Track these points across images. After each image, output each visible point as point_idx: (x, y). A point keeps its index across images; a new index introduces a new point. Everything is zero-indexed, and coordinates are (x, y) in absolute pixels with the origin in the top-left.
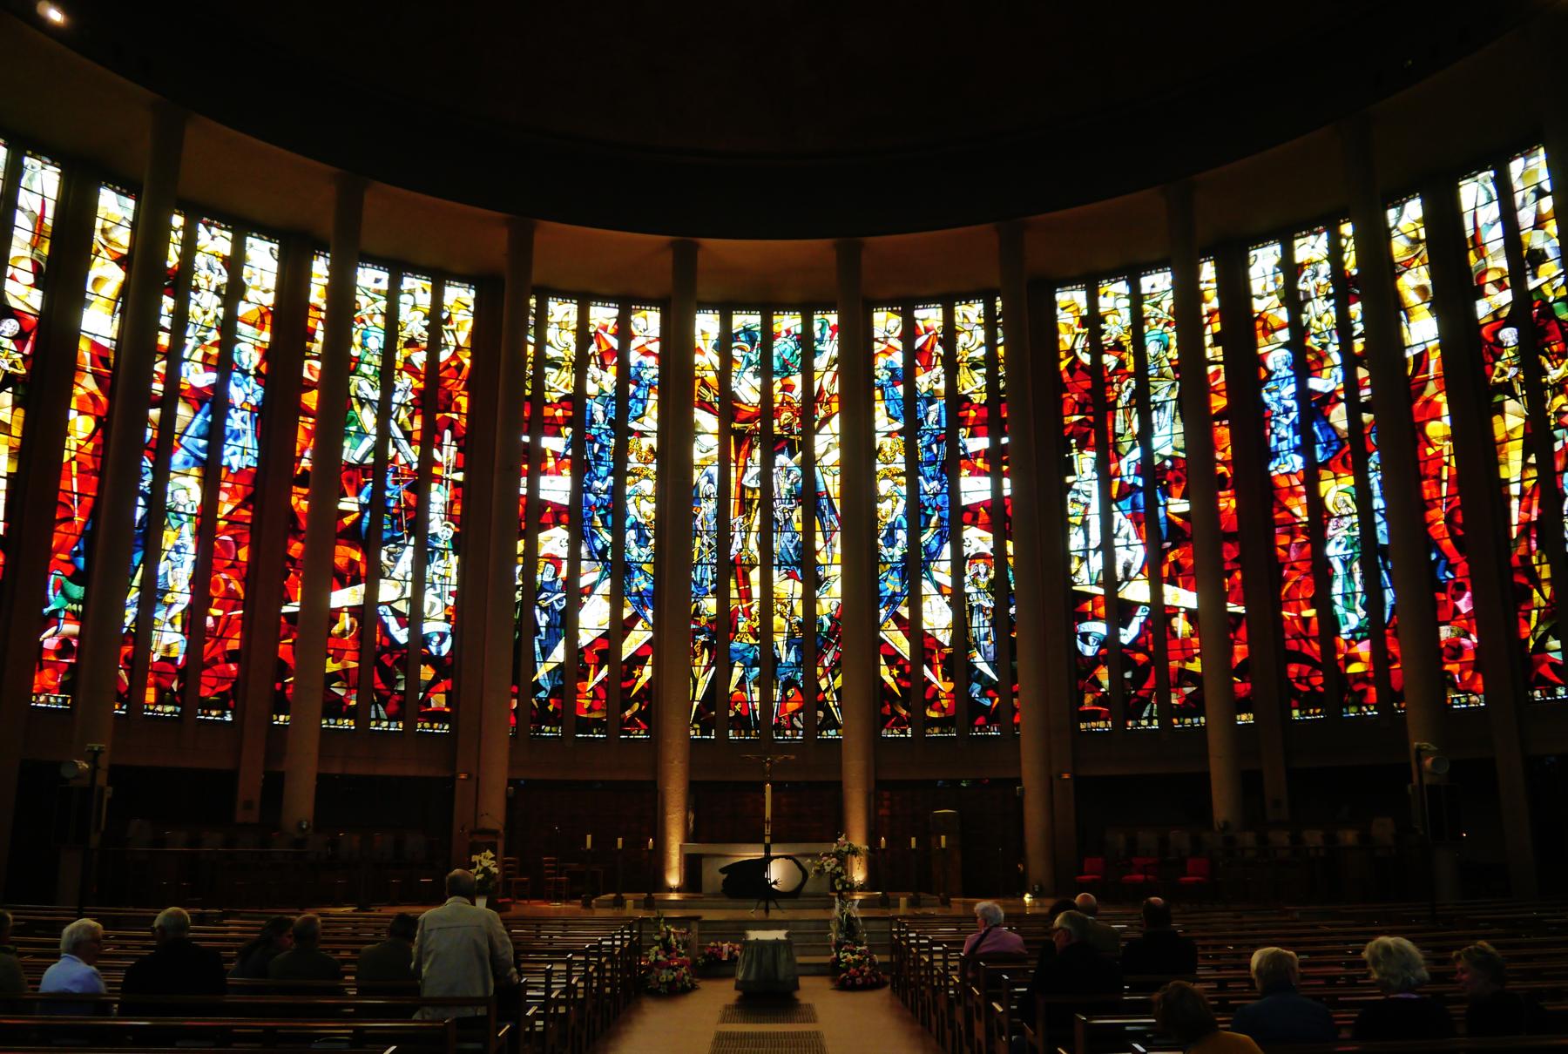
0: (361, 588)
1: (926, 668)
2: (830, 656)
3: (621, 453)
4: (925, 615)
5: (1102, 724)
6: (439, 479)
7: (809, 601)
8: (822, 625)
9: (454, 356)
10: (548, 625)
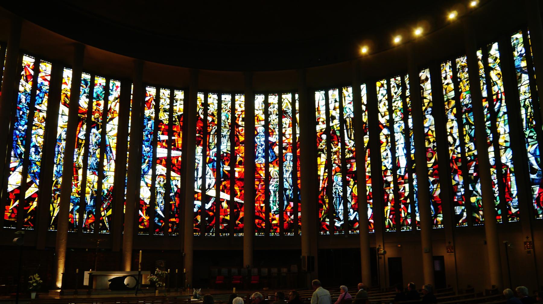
1: (140, 211)
2: (106, 203)
3: (31, 117)
4: (141, 193)
5: (197, 234)
7: (100, 183)
8: (104, 193)
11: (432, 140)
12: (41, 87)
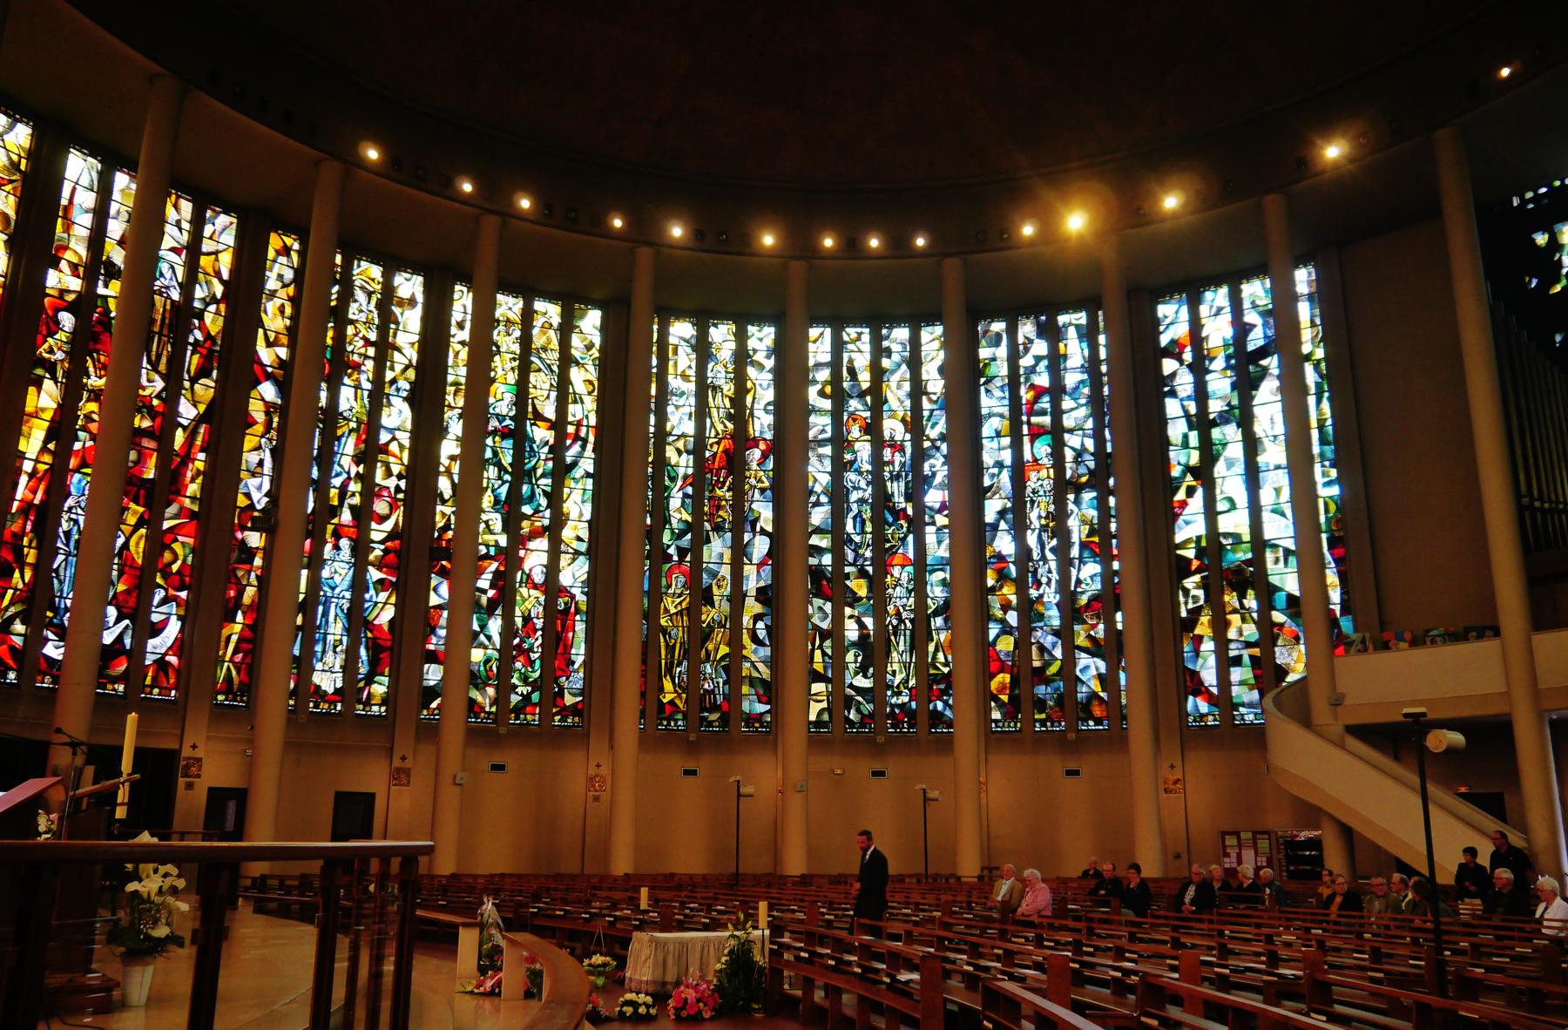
11: (396, 469)
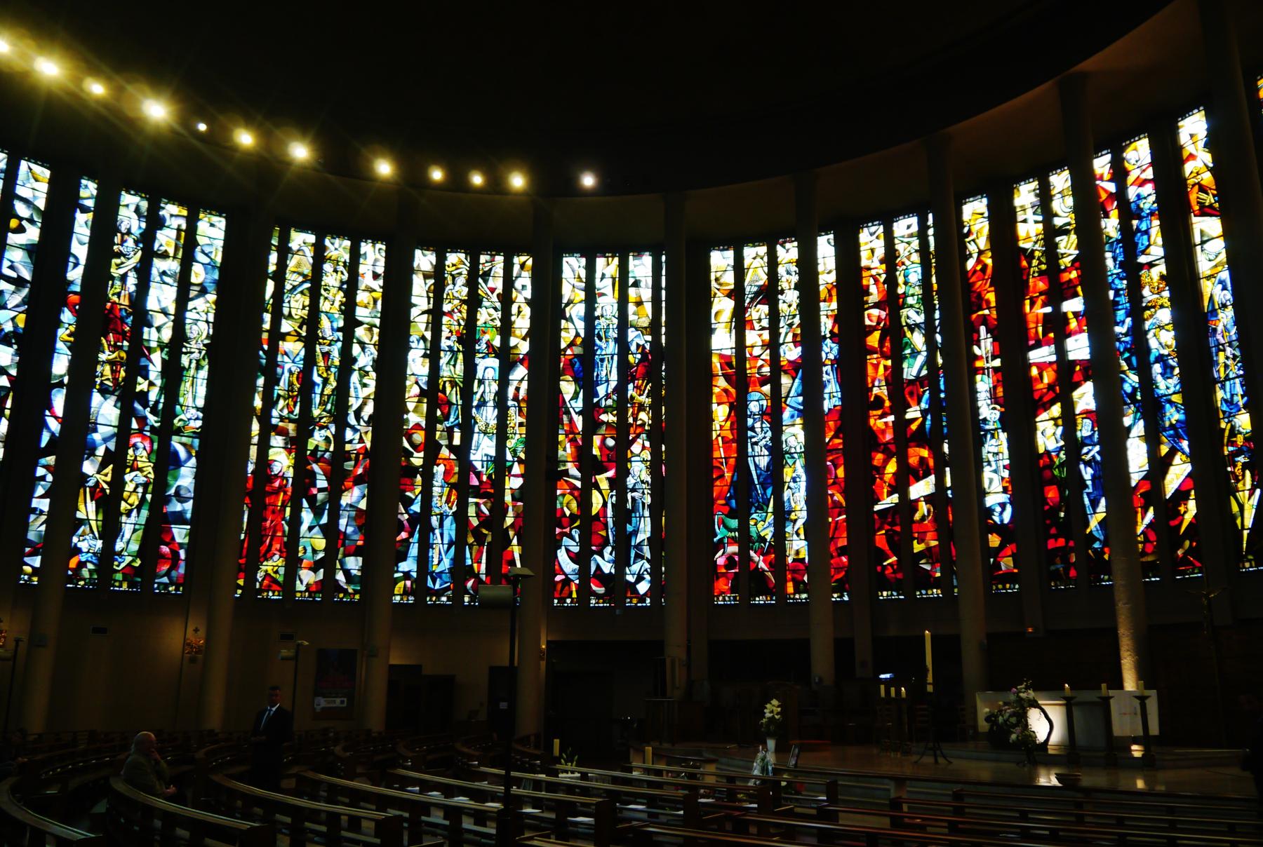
0: (932, 478)
6: (982, 370)
9: (979, 261)
10: (1094, 478)
12: (1138, 206)
